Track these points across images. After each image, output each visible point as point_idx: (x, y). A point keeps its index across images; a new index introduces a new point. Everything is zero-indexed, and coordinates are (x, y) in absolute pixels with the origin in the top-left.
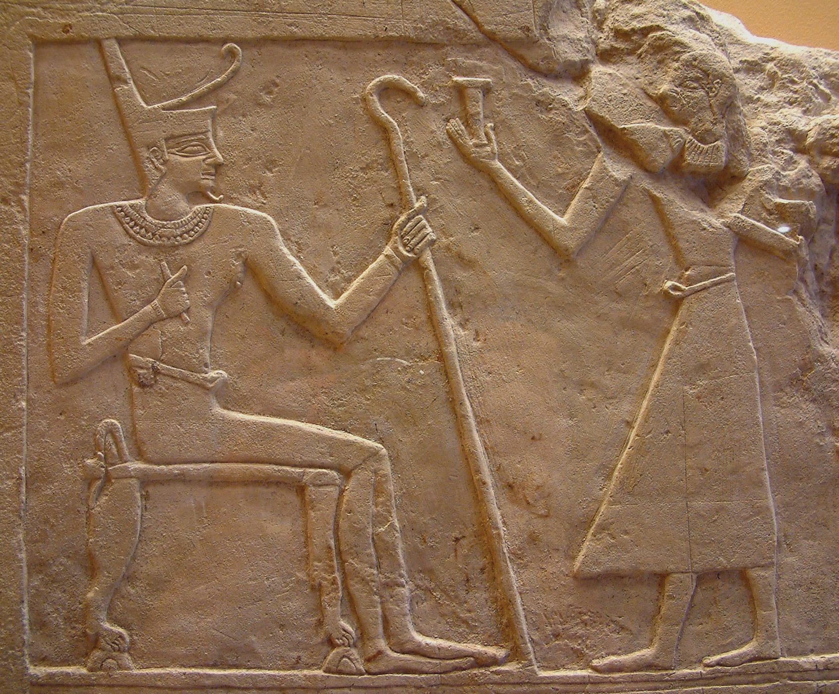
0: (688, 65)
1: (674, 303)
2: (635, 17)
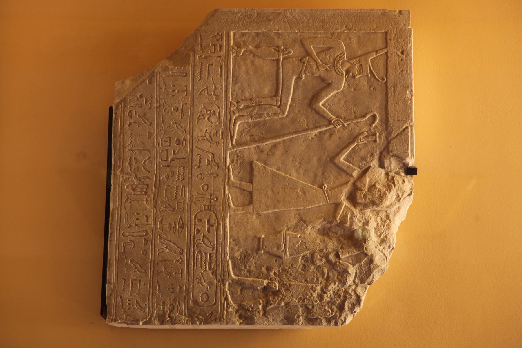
0: (384, 193)
1: (321, 186)
2: (398, 181)
